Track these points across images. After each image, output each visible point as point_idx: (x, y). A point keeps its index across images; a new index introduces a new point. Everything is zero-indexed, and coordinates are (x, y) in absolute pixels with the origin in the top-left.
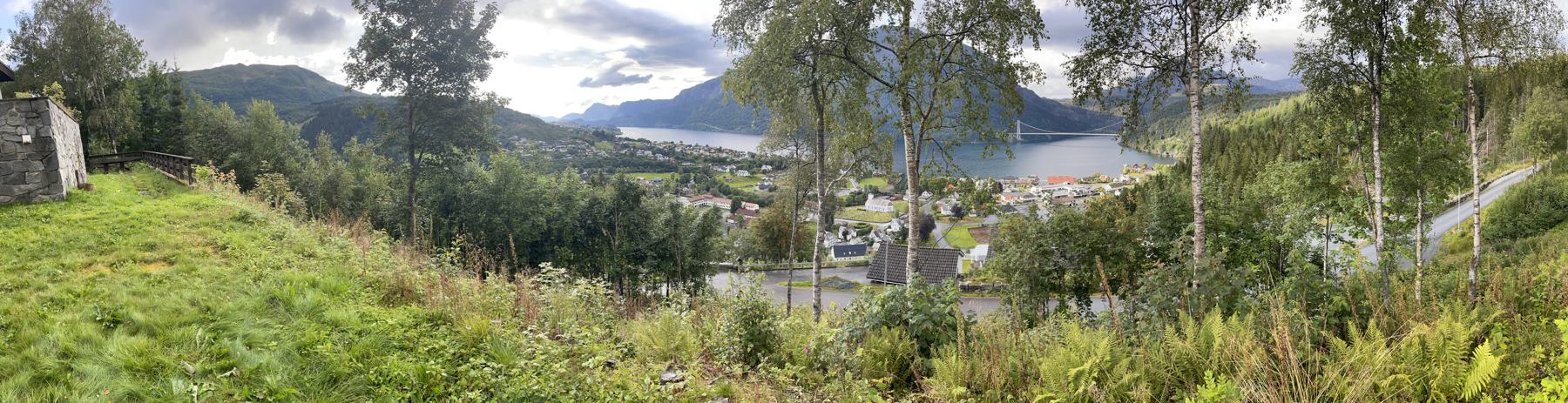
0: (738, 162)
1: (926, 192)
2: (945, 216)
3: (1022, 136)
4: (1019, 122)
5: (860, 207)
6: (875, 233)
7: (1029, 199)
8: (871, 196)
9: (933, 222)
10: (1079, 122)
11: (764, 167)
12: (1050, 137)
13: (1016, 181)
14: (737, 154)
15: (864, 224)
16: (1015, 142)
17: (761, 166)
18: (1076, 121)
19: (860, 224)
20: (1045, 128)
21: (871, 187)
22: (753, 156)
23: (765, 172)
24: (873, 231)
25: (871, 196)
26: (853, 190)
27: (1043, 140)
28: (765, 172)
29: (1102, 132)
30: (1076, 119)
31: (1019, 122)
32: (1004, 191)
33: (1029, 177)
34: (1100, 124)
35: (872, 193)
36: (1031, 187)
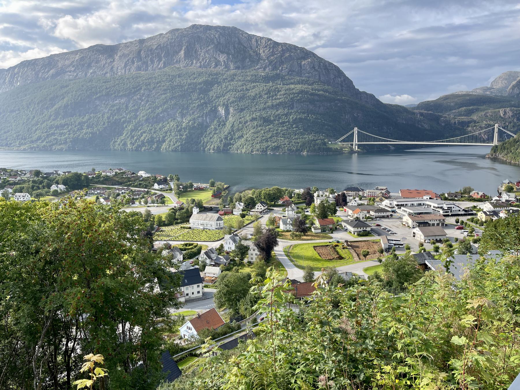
0: (15, 184)
7: (382, 214)
11: (54, 187)
12: (392, 148)
13: (361, 193)
14: (15, 173)
16: (352, 152)
17: (49, 186)
22: (37, 173)
23: (56, 194)
27: (384, 151)
28: (56, 194)
30: (426, 126)
32: (350, 204)
33: (377, 189)
36: (381, 200)
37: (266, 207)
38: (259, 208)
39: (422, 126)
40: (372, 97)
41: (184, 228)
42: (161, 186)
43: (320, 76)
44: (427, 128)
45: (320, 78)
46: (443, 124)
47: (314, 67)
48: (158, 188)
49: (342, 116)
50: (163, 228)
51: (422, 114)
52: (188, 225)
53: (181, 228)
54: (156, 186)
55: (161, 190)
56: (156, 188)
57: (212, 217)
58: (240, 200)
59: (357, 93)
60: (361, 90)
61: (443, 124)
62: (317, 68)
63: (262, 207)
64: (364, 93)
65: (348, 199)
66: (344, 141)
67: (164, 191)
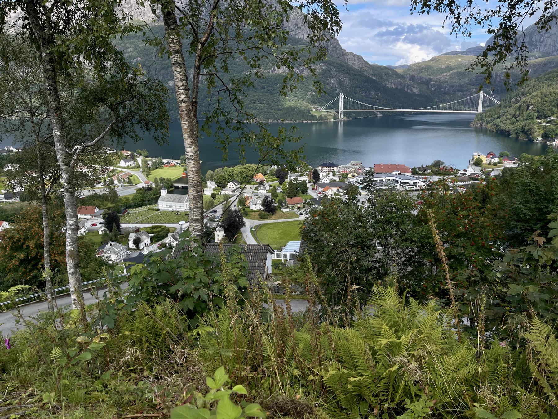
1: (231, 183)
2: (255, 211)
3: (345, 114)
4: (341, 95)
5: (152, 206)
6: (173, 237)
8: (164, 193)
9: (241, 218)
10: (418, 95)
15: (160, 227)
18: (415, 95)
19: (153, 228)
20: (374, 102)
21: (162, 180)
24: (170, 235)
25: (164, 193)
26: (140, 186)
29: (450, 108)
30: (415, 91)
31: (341, 95)
34: (448, 98)
35: (166, 188)
37: (239, 186)
38: (232, 187)
39: (412, 91)
40: (360, 58)
41: (153, 210)
42: (128, 164)
43: (303, 35)
44: (417, 93)
45: (304, 37)
46: (433, 89)
47: (297, 25)
48: (125, 166)
49: (328, 80)
50: (131, 211)
51: (412, 78)
52: (157, 208)
53: (149, 209)
54: (122, 163)
55: (128, 168)
56: (122, 166)
57: (181, 198)
58: (212, 179)
59: (344, 54)
60: (348, 51)
61: (433, 89)
62: (300, 25)
63: (234, 186)
64: (352, 54)
65: (321, 176)
66: (329, 108)
67: (131, 168)
